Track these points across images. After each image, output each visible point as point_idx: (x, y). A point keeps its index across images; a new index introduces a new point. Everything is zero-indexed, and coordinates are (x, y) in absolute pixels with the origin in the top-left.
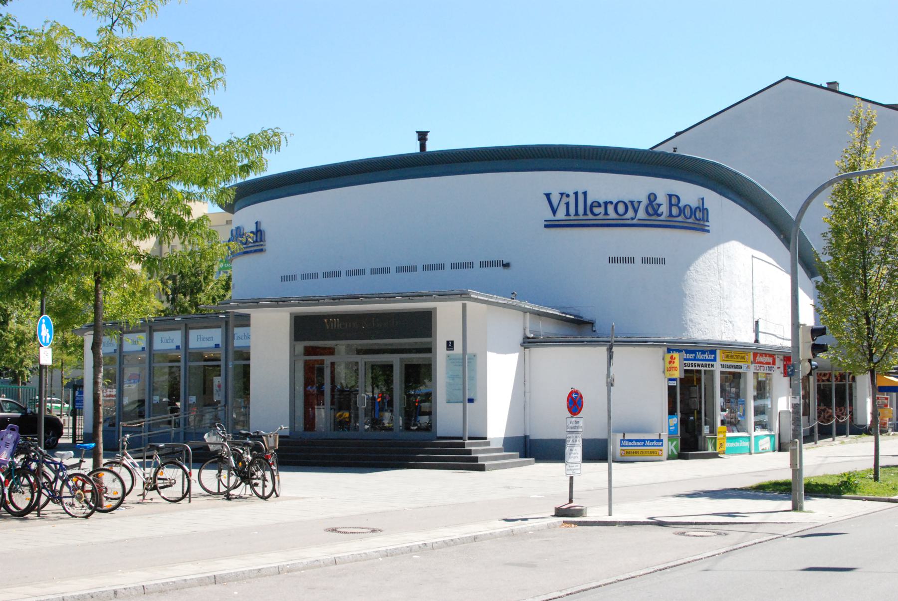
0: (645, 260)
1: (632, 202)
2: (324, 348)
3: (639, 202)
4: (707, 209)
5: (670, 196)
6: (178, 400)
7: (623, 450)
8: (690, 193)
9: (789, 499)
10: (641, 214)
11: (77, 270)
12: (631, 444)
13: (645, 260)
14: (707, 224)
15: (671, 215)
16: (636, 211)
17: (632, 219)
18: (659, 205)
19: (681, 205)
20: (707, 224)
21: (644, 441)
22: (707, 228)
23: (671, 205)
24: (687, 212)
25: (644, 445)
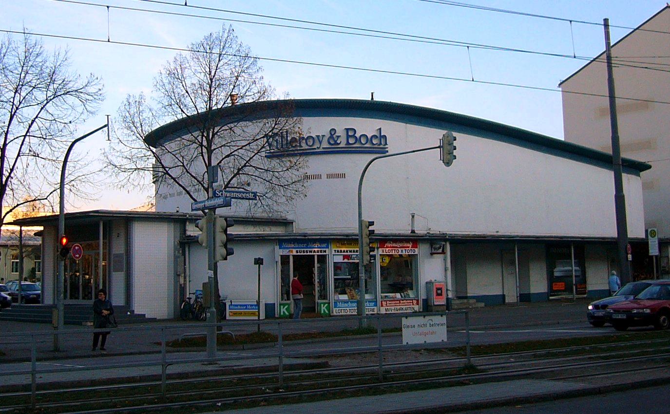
0: (329, 176)
1: (318, 136)
2: (103, 282)
3: (323, 136)
4: (385, 137)
5: (347, 130)
6: (103, 265)
7: (231, 312)
8: (366, 126)
9: (630, 239)
10: (325, 144)
11: (143, 110)
12: (236, 308)
13: (329, 176)
14: (387, 146)
15: (348, 143)
16: (320, 143)
17: (318, 148)
18: (338, 137)
19: (358, 135)
20: (387, 146)
21: (246, 305)
22: (387, 150)
23: (348, 136)
24: (363, 141)
25: (246, 309)
